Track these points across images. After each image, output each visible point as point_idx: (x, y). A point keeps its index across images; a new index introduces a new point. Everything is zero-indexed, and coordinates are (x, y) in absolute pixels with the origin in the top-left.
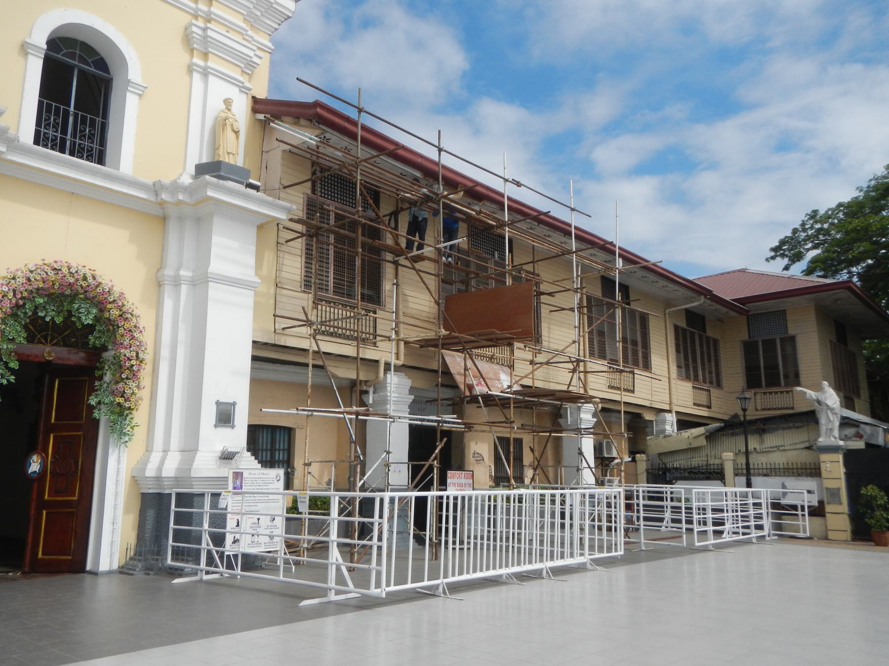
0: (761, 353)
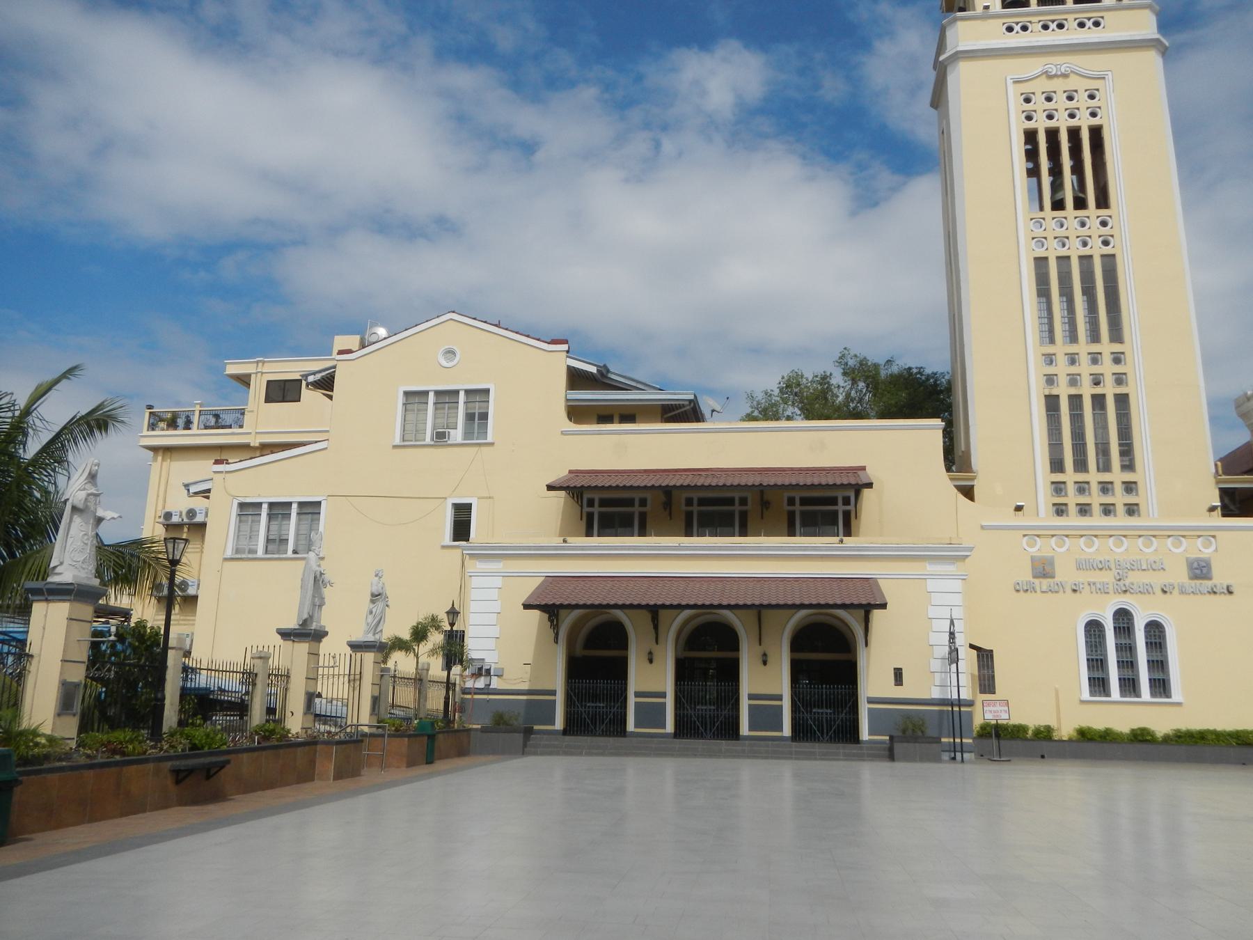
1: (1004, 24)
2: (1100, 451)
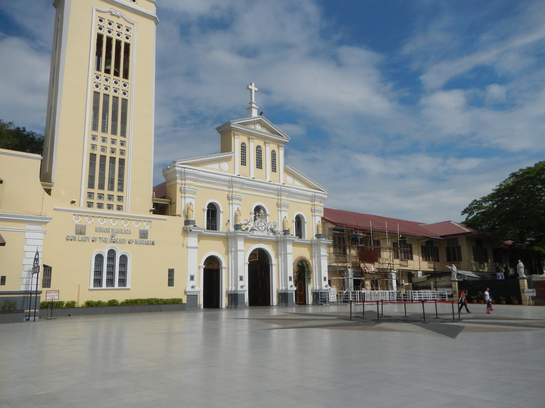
0: (451, 251)
2: (110, 182)
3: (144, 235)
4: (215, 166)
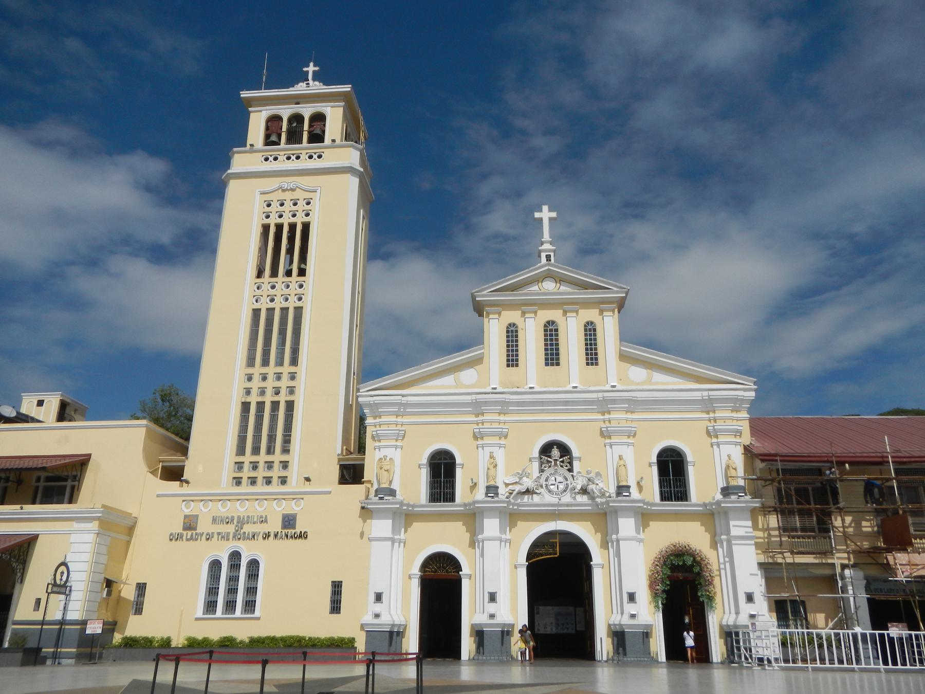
1: (263, 156)
3: (289, 521)
4: (449, 380)
